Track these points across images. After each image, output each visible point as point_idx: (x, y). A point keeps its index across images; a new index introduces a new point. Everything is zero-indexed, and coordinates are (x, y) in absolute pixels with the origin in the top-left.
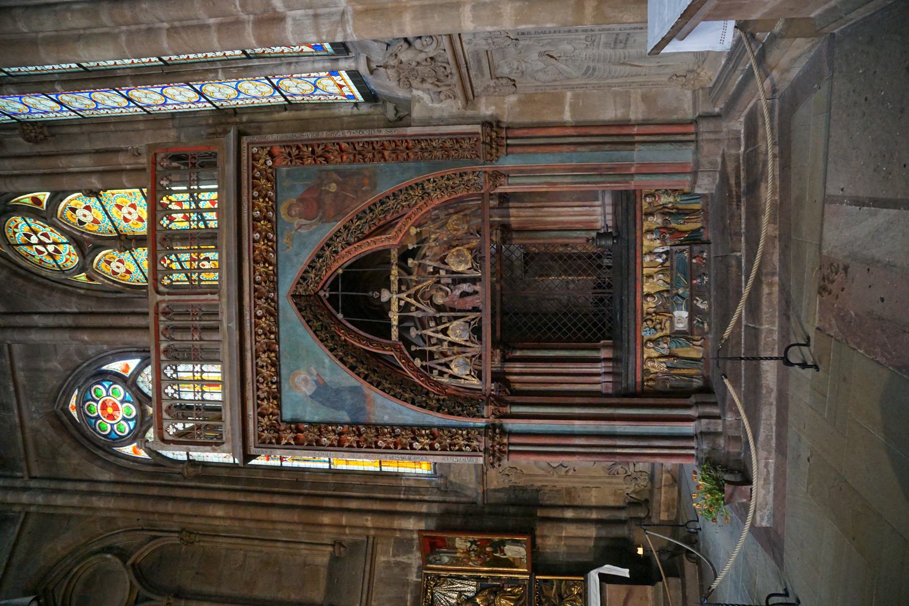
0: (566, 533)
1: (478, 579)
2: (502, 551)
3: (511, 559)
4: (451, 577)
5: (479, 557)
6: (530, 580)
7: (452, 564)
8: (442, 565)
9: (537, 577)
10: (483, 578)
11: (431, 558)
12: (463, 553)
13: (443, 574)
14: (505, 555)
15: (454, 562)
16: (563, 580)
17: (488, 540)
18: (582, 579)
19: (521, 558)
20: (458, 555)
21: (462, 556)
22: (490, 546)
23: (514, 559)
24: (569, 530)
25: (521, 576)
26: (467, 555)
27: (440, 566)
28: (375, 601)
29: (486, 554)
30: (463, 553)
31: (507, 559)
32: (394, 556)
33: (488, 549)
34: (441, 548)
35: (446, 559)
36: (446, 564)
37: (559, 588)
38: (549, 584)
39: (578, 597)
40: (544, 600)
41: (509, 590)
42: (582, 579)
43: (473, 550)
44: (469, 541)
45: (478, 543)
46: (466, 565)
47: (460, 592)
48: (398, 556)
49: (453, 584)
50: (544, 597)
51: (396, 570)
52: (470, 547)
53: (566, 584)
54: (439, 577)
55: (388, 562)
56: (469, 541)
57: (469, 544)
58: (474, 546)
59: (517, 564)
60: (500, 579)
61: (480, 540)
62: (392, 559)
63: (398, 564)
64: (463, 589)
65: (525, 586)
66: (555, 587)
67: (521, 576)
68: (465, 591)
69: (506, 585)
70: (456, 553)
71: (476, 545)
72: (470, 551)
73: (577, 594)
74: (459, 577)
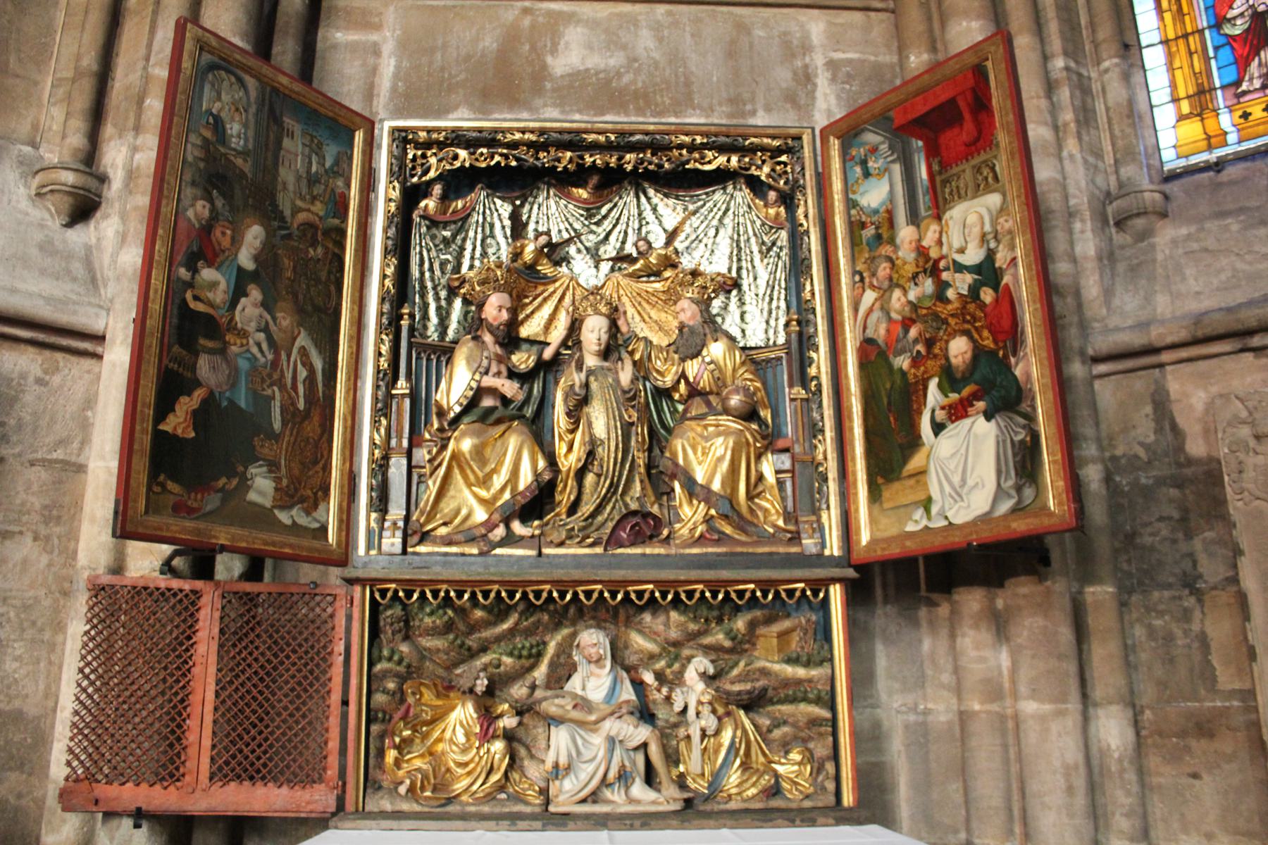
0: (1042, 719)
1: (802, 342)
2: (957, 412)
3: (915, 462)
4: (796, 238)
5: (907, 323)
6: (818, 559)
7: (855, 227)
8: (846, 189)
9: (836, 594)
10: (804, 363)
11: (871, 138)
12: (922, 252)
13: (807, 208)
14: (938, 428)
15: (869, 232)
16: (833, 707)
17: (1011, 335)
18: (848, 799)
19: (927, 504)
20: (906, 233)
21: (906, 253)
22: (978, 353)
23: (922, 472)
24: (1055, 727)
25: (831, 518)
26: (910, 269)
27: (837, 185)
28: (669, 13)
29: (930, 343)
30: (922, 252)
31: (913, 442)
32: (832, 65)
33: (959, 348)
34: (932, 151)
35: (874, 195)
36: (851, 204)
37: (795, 692)
38: (811, 646)
39: (766, 780)
40: (740, 624)
41: (770, 478)
42: (848, 799)
43: (942, 286)
44: (991, 255)
45: (987, 295)
46: (860, 281)
47: (736, 284)
48: (833, 80)
49: (764, 255)
50: (752, 625)
51: (783, 76)
52: (959, 268)
53: (814, 722)
54: (788, 200)
55: (806, 48)
56: (991, 255)
57: (973, 256)
58: (962, 283)
59: (896, 493)
60: (815, 430)
61: (1007, 300)
62: (819, 60)
63: (806, 78)
64: (749, 297)
65: (796, 538)
66: (801, 672)
67: (831, 518)
68: (742, 303)
69: (785, 461)
70: (914, 218)
71: (974, 291)
72: (934, 270)
73: (777, 776)
74: (798, 267)
